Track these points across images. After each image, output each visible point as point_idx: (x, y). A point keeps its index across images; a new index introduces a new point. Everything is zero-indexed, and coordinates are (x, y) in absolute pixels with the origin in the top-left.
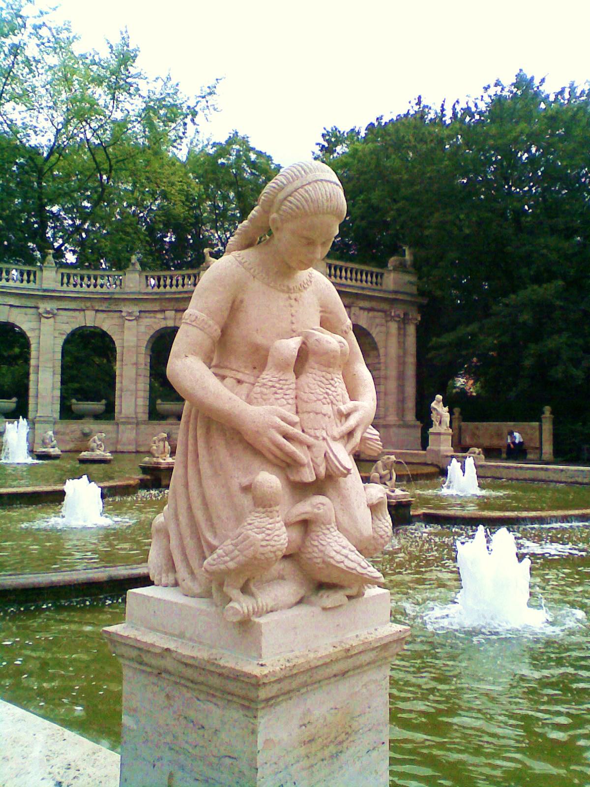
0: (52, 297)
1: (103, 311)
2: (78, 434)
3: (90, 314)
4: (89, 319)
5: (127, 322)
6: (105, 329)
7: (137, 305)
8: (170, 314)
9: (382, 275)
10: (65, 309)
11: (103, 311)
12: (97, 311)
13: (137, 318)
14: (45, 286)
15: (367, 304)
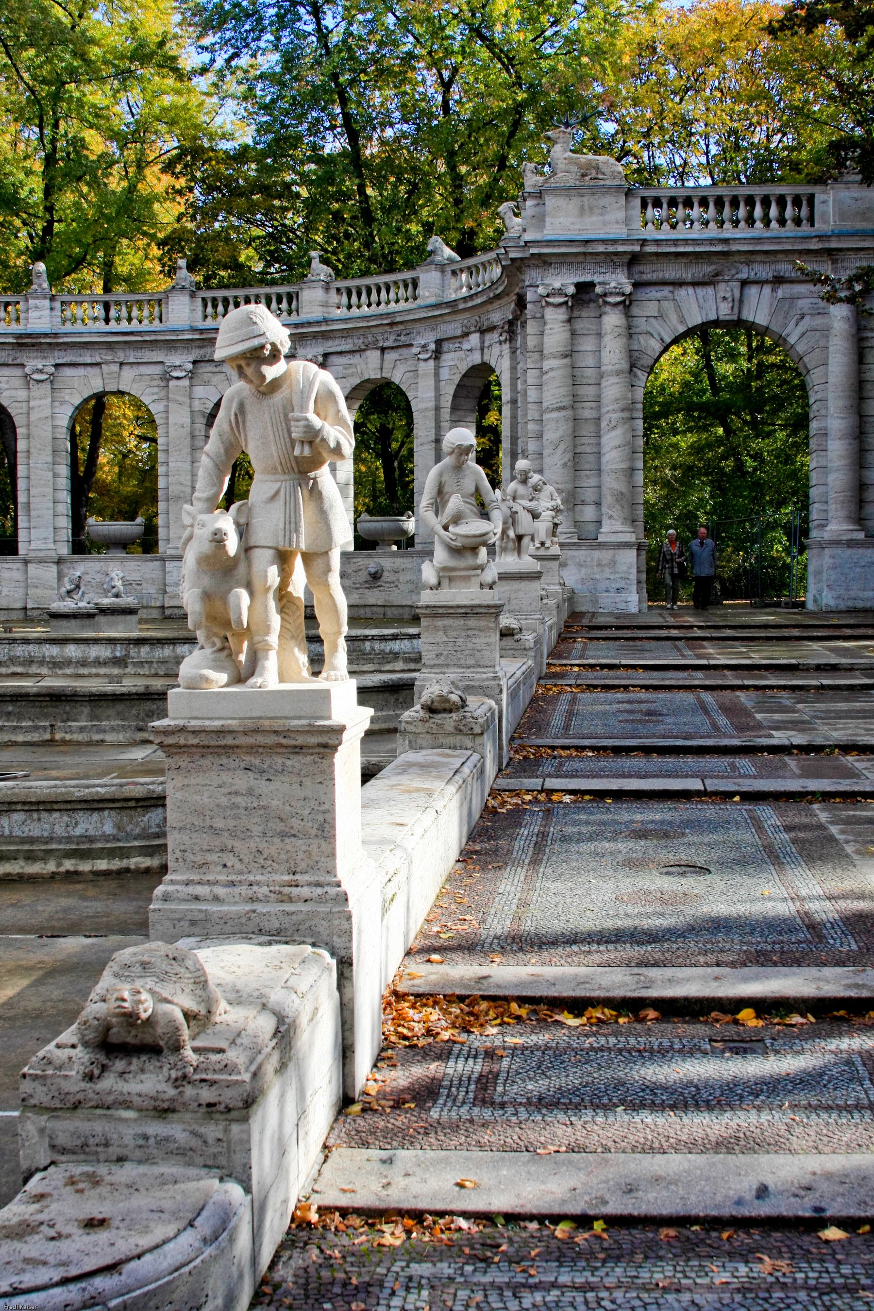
0: (315, 336)
1: (392, 348)
2: (363, 576)
3: (373, 356)
4: (370, 367)
5: (422, 364)
6: (397, 381)
7: (433, 329)
8: (475, 338)
9: (811, 199)
10: (341, 353)
11: (392, 348)
12: (383, 350)
13: (437, 354)
14: (304, 316)
15: (763, 271)
